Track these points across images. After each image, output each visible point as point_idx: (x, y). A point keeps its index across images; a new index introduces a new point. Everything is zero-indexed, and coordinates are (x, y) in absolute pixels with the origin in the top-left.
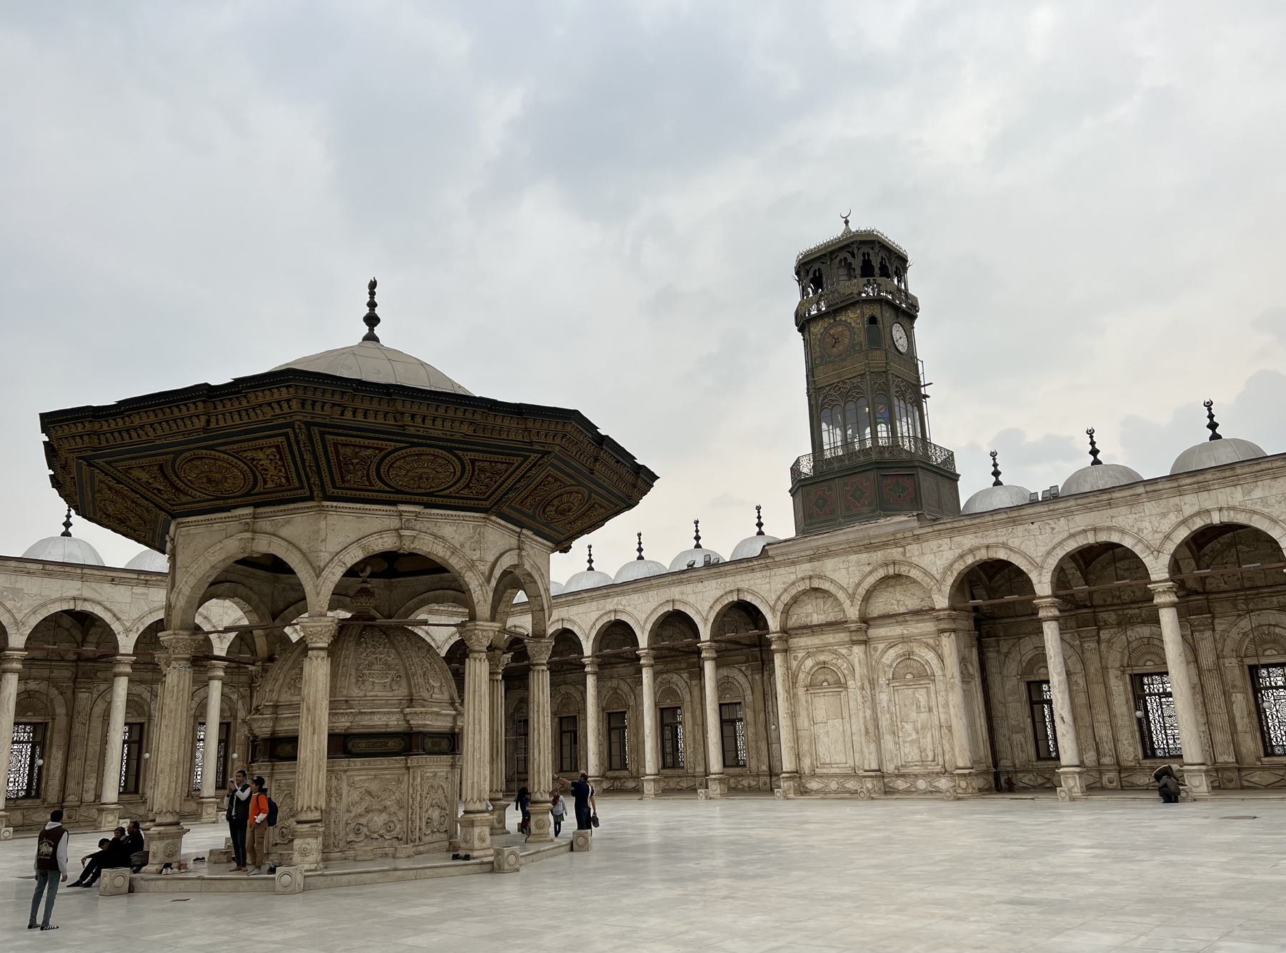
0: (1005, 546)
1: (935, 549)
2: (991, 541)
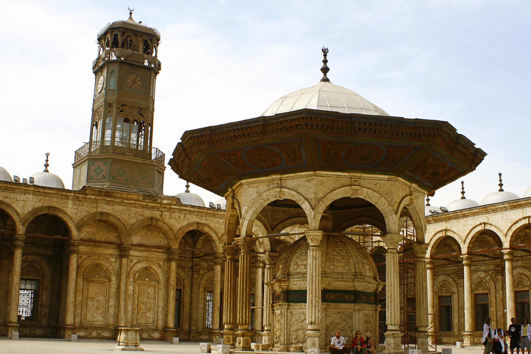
0: (208, 225)
1: (177, 218)
2: (203, 222)
